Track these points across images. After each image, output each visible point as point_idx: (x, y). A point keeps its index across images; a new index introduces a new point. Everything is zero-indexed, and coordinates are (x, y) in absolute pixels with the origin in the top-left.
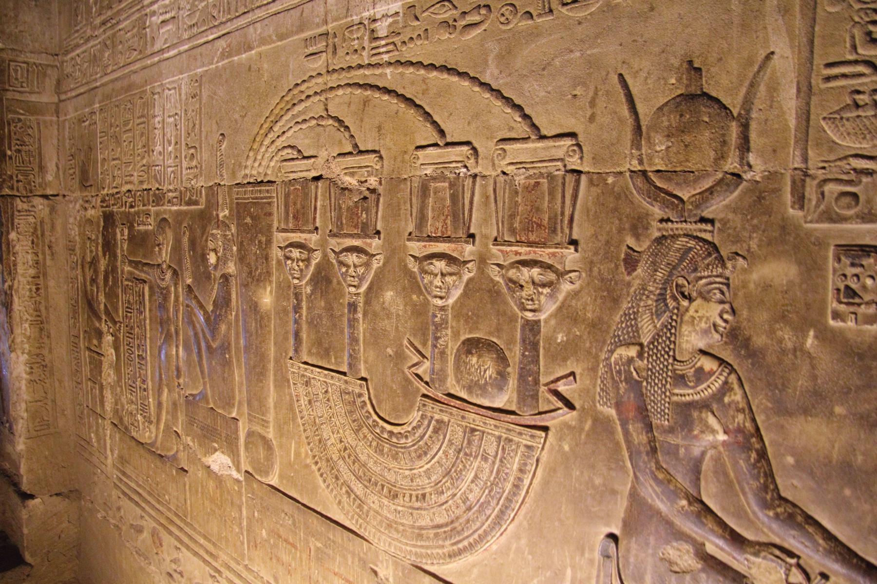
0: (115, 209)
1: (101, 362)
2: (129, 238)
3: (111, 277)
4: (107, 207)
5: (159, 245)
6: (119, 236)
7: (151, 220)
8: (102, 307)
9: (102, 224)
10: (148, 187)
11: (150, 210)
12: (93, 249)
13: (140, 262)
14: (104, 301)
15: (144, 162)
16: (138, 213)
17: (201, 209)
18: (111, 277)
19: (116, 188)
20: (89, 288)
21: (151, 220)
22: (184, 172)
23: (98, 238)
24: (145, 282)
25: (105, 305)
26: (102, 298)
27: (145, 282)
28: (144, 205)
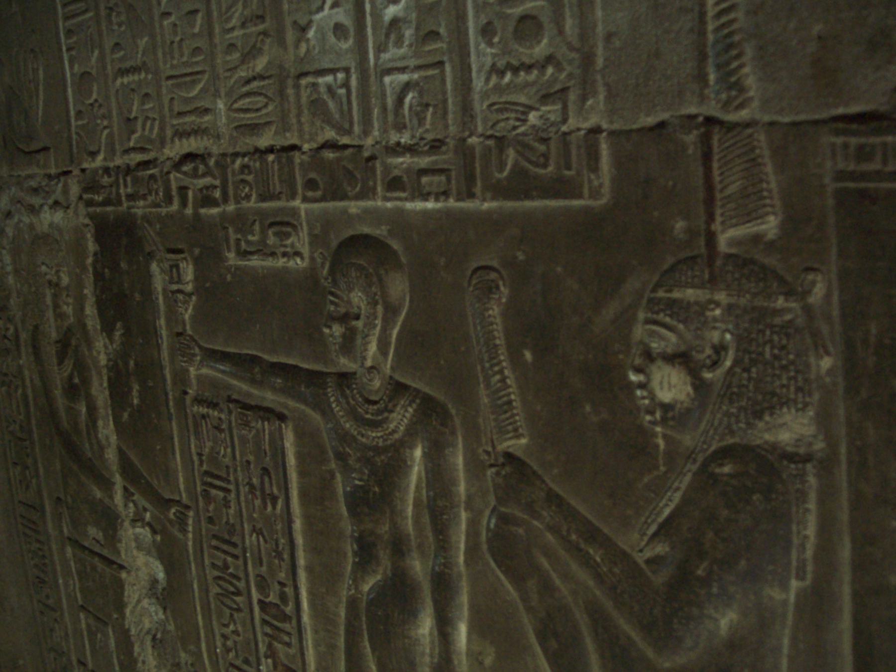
0: (140, 208)
1: (120, 585)
2: (197, 291)
3: (136, 387)
4: (107, 202)
5: (345, 318)
6: (159, 282)
7: (301, 241)
8: (111, 455)
9: (92, 246)
10: (280, 142)
11: (295, 212)
12: (69, 310)
13: (254, 359)
14: (114, 438)
15: (260, 64)
16: (241, 221)
17: (587, 210)
18: (136, 387)
19: (143, 150)
20: (61, 402)
21: (301, 241)
22: (478, 83)
23: (80, 285)
24: (282, 418)
25: (121, 452)
26: (107, 431)
27: (282, 418)
28: (263, 198)
